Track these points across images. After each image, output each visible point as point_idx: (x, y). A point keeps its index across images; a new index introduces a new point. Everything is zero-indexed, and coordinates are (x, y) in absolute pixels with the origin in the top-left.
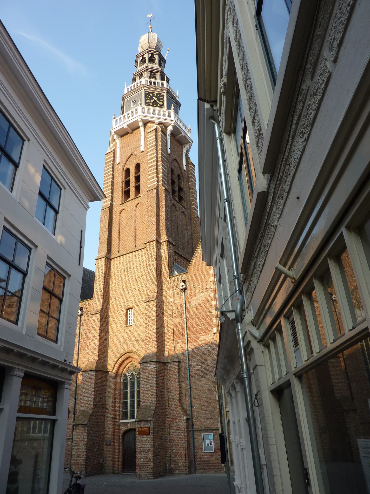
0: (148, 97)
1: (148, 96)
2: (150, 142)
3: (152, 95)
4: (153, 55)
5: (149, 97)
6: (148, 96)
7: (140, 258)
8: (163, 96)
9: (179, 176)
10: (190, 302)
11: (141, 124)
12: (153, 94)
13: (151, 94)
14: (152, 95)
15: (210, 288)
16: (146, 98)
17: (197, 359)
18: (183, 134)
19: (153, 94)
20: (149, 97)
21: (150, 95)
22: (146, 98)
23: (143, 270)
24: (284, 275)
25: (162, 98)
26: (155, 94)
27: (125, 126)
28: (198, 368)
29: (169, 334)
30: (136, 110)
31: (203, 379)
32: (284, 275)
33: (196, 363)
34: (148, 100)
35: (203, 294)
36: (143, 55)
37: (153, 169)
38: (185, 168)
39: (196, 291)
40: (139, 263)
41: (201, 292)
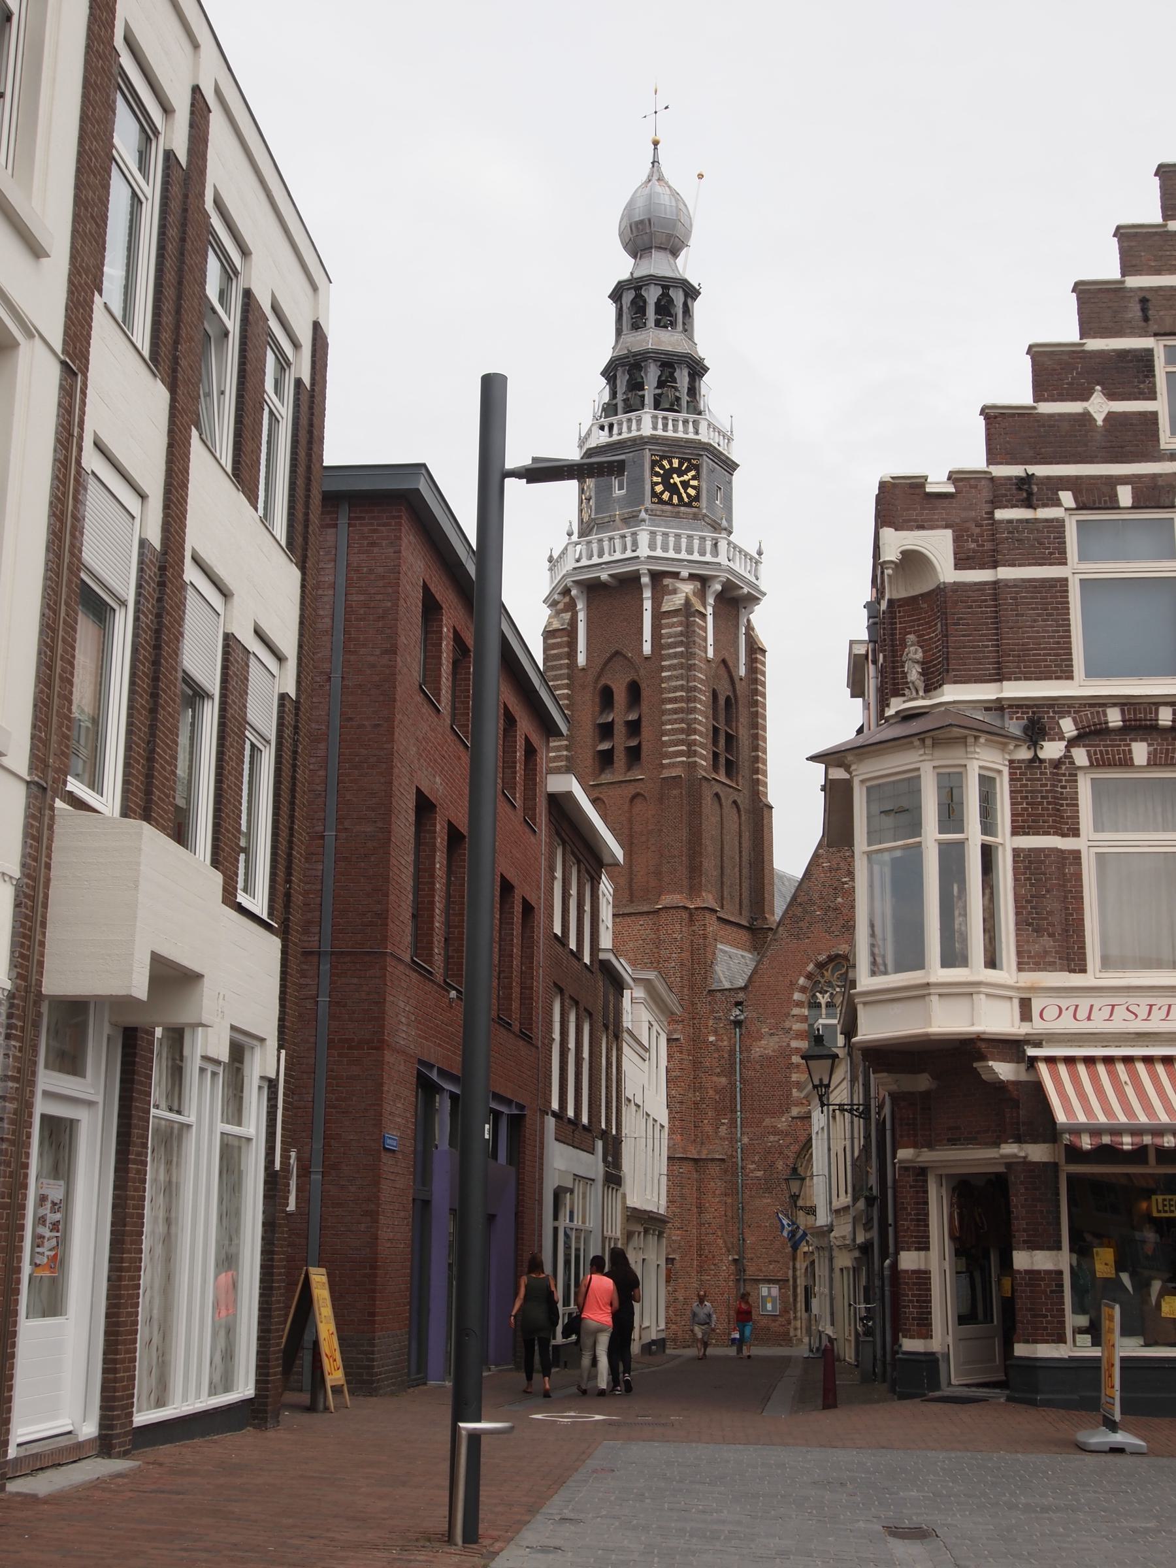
0: (657, 474)
1: (657, 469)
2: (670, 640)
3: (667, 467)
4: (666, 288)
5: (662, 472)
6: (657, 469)
7: (641, 932)
8: (697, 468)
9: (728, 699)
10: (749, 1050)
11: (645, 580)
12: (671, 463)
13: (665, 463)
14: (667, 467)
15: (790, 1029)
16: (655, 479)
17: (756, 1158)
18: (746, 590)
19: (671, 463)
20: (662, 472)
21: (662, 467)
22: (655, 479)
23: (649, 961)
24: (1129, 487)
25: (693, 473)
26: (676, 463)
27: (604, 576)
28: (760, 1174)
29: (704, 1106)
30: (634, 534)
31: (767, 1195)
32: (1129, 487)
33: (754, 1166)
34: (657, 484)
35: (776, 1038)
36: (640, 288)
37: (676, 719)
38: (742, 671)
39: (763, 1030)
40: (641, 942)
41: (772, 1034)
